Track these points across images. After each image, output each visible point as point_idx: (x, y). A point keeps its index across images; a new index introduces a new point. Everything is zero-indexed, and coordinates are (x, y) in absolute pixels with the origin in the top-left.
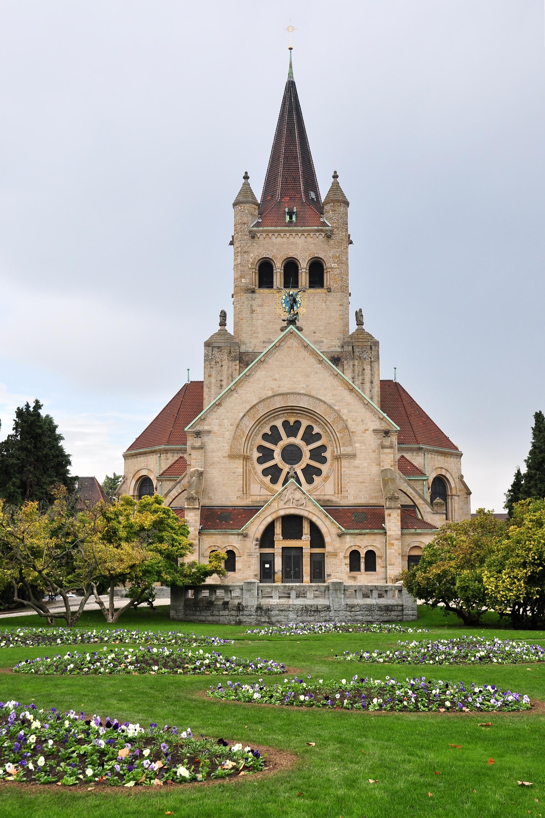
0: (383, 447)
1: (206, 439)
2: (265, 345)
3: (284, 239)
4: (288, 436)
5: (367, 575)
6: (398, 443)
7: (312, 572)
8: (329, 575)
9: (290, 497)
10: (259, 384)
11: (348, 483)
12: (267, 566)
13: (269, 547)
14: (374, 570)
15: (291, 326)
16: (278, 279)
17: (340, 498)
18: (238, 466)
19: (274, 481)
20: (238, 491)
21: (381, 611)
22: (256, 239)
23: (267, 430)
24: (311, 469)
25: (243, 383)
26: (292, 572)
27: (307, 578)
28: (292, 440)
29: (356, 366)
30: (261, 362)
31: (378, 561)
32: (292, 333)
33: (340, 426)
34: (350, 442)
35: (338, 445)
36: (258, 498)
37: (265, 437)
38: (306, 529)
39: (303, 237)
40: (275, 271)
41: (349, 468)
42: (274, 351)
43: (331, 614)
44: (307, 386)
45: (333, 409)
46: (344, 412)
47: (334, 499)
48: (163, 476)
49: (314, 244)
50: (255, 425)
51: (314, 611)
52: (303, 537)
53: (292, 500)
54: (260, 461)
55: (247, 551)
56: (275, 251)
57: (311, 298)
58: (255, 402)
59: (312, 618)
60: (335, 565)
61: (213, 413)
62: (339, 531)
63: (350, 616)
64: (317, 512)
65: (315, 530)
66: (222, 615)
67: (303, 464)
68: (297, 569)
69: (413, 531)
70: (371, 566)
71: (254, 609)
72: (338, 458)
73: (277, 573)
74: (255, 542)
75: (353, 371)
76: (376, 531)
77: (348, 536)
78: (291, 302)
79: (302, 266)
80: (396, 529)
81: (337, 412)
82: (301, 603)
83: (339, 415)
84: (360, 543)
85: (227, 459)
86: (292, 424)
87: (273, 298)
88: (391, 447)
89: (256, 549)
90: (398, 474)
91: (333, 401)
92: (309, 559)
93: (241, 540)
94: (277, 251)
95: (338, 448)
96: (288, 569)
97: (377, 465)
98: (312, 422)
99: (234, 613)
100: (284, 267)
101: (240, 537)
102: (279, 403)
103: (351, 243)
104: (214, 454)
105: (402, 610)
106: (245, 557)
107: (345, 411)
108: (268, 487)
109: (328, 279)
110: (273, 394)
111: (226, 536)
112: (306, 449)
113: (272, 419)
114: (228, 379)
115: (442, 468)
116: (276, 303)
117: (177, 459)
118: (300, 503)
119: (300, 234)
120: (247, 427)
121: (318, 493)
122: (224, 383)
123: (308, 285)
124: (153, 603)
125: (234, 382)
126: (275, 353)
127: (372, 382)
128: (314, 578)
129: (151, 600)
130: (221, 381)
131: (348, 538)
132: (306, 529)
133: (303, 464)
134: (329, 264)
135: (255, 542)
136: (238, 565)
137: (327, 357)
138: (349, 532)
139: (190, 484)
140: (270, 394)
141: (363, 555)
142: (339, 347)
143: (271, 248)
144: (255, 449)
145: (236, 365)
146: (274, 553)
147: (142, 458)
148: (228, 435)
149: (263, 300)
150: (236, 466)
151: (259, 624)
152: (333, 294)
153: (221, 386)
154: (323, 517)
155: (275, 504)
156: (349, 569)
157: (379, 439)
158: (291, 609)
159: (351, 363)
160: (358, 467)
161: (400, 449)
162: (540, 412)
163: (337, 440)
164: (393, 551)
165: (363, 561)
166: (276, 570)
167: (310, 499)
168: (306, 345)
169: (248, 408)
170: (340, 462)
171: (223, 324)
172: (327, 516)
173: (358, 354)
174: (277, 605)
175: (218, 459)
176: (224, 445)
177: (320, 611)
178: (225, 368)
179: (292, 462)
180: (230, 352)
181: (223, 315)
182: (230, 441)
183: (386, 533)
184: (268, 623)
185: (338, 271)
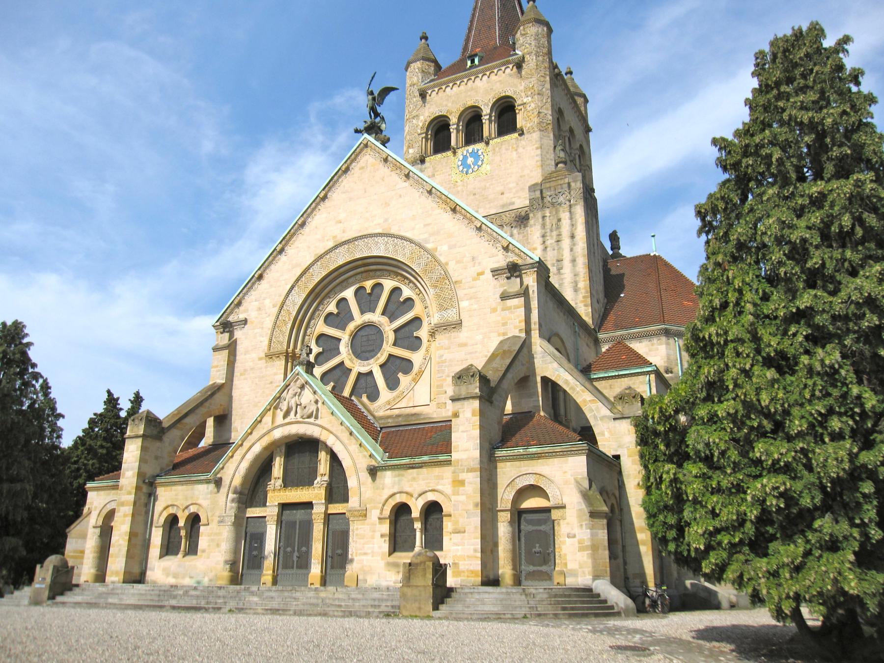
3: (463, 87)
4: (362, 312)
9: (293, 403)
23: (332, 308)
24: (398, 362)
27: (316, 569)
39: (485, 78)
41: (449, 348)
42: (340, 180)
44: (386, 220)
45: (425, 250)
49: (500, 81)
50: (309, 301)
55: (217, 514)
56: (450, 105)
57: (497, 149)
69: (521, 451)
74: (231, 496)
75: (544, 226)
77: (388, 474)
81: (431, 254)
83: (433, 257)
85: (264, 361)
87: (447, 163)
91: (426, 236)
94: (452, 103)
96: (289, 549)
102: (342, 258)
106: (214, 525)
111: (190, 487)
113: (337, 289)
116: (451, 168)
121: (402, 404)
128: (332, 567)
131: (388, 478)
135: (231, 496)
136: (203, 543)
140: (331, 244)
141: (416, 513)
143: (445, 103)
148: (269, 323)
149: (434, 169)
152: (526, 136)
154: (345, 436)
159: (539, 215)
160: (465, 345)
166: (266, 553)
173: (549, 199)
179: (367, 355)
185: (533, 105)
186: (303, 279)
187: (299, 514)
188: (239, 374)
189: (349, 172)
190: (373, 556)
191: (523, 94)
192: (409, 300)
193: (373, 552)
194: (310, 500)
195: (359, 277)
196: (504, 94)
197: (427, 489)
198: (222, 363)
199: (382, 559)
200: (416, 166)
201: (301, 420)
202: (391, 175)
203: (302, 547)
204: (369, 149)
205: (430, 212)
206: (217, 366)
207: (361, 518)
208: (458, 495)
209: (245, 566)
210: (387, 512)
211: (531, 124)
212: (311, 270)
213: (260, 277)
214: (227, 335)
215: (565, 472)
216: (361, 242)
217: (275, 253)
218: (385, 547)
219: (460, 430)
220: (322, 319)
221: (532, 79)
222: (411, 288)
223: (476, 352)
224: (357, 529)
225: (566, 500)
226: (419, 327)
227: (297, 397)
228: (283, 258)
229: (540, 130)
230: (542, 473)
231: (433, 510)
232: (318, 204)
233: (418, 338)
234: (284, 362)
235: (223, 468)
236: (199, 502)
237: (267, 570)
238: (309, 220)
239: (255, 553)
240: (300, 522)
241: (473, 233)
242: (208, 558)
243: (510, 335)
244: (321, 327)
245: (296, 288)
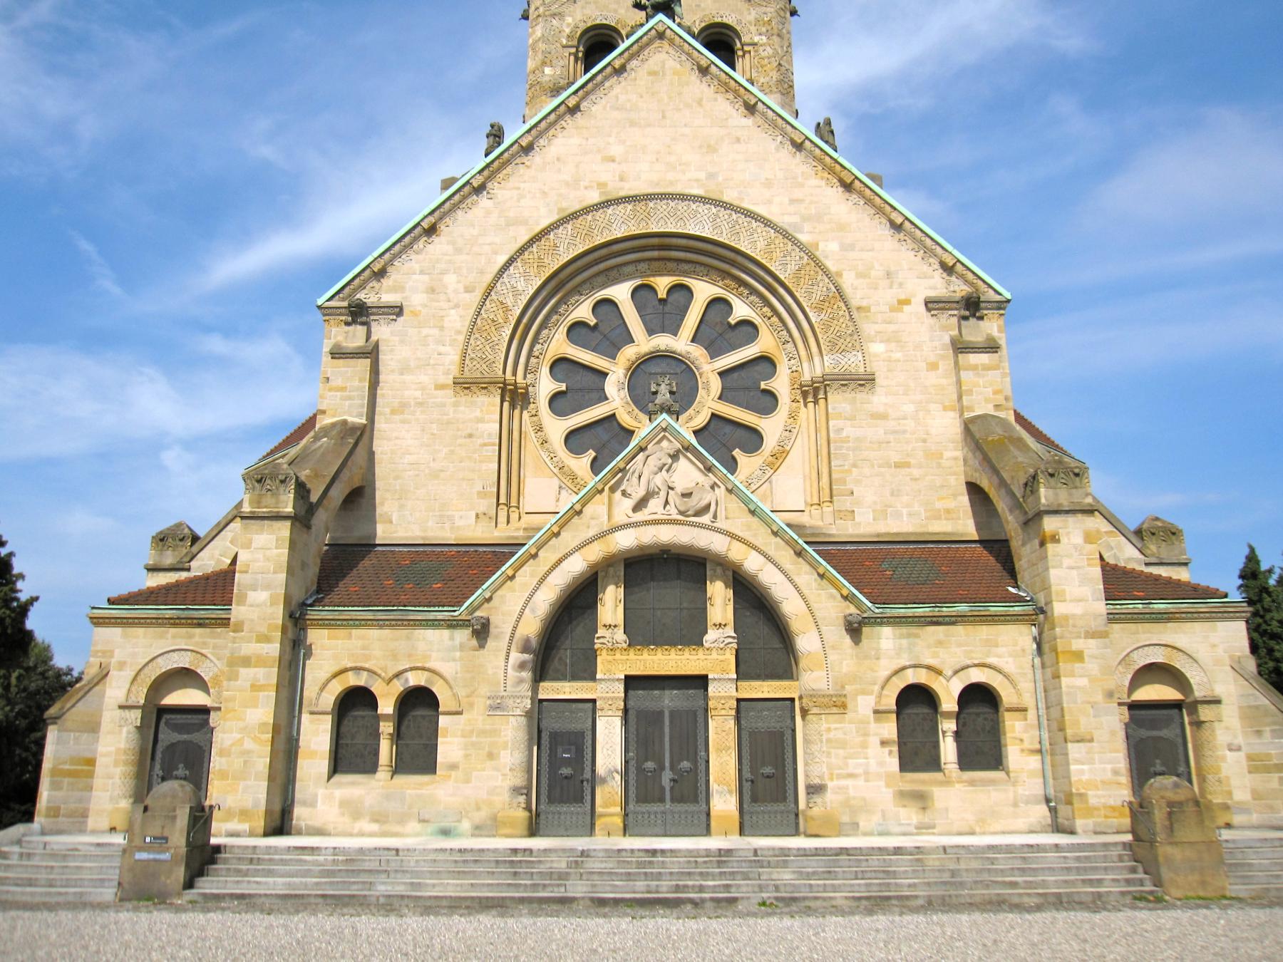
1: (382, 331)
4: (651, 331)
5: (972, 783)
7: (747, 775)
8: (815, 790)
9: (659, 480)
10: (559, 171)
11: (855, 466)
13: (575, 677)
17: (829, 519)
20: (482, 494)
23: (583, 311)
24: (728, 429)
25: (509, 169)
26: (667, 776)
27: (724, 802)
28: (663, 341)
32: (661, 36)
33: (822, 287)
34: (853, 339)
41: (852, 418)
42: (607, 84)
44: (711, 176)
45: (796, 243)
46: (829, 251)
50: (544, 293)
52: (711, 636)
53: (663, 494)
55: (484, 690)
58: (545, 223)
60: (842, 744)
61: (413, 256)
62: (852, 610)
68: (685, 764)
69: (1139, 606)
72: (812, 392)
73: (604, 781)
74: (516, 656)
76: (995, 609)
77: (887, 631)
80: (1086, 591)
83: (812, 257)
84: (935, 655)
85: (450, 392)
86: (662, 294)
89: (521, 681)
92: (731, 723)
93: (462, 647)
96: (650, 765)
98: (726, 287)
101: (463, 635)
102: (620, 225)
104: (408, 378)
106: (476, 716)
110: (604, 199)
111: (402, 633)
112: (709, 369)
113: (601, 279)
118: (696, 502)
120: (516, 293)
128: (755, 799)
131: (886, 639)
135: (516, 656)
136: (448, 748)
138: (889, 612)
140: (594, 197)
141: (949, 703)
144: (545, 370)
146: (594, 701)
148: (458, 321)
150: (478, 413)
157: (945, 328)
160: (883, 417)
164: (1083, 682)
166: (601, 768)
169: (525, 238)
170: (822, 402)
175: (418, 394)
176: (442, 349)
182: (461, 338)
185: (769, 51)
186: (534, 249)
187: (669, 699)
188: (387, 410)
189: (625, 75)
190: (867, 780)
191: (753, 29)
192: (746, 323)
193: (867, 773)
194: (704, 673)
196: (719, 20)
197: (969, 662)
198: (356, 383)
199: (887, 785)
200: (772, 96)
201: (680, 517)
202: (716, 100)
203: (646, 760)
204: (665, 43)
205: (800, 180)
206: (343, 389)
207: (835, 710)
208: (1074, 676)
209: (544, 798)
210: (891, 702)
211: (767, 79)
212: (552, 236)
213: (431, 231)
214: (361, 330)
215: (1214, 646)
216: (662, 205)
217: (467, 189)
218: (894, 762)
219: (1065, 565)
220: (563, 330)
221: (768, 10)
223: (904, 432)
224: (829, 730)
225: (1220, 690)
227: (664, 472)
228: (483, 202)
229: (783, 94)
230: (1177, 645)
232: (560, 117)
233: (770, 394)
234: (498, 400)
235: (489, 600)
237: (606, 805)
238: (542, 142)
239: (566, 771)
240: (672, 713)
241: (887, 231)
242: (468, 781)
244: (559, 344)
245: (519, 263)
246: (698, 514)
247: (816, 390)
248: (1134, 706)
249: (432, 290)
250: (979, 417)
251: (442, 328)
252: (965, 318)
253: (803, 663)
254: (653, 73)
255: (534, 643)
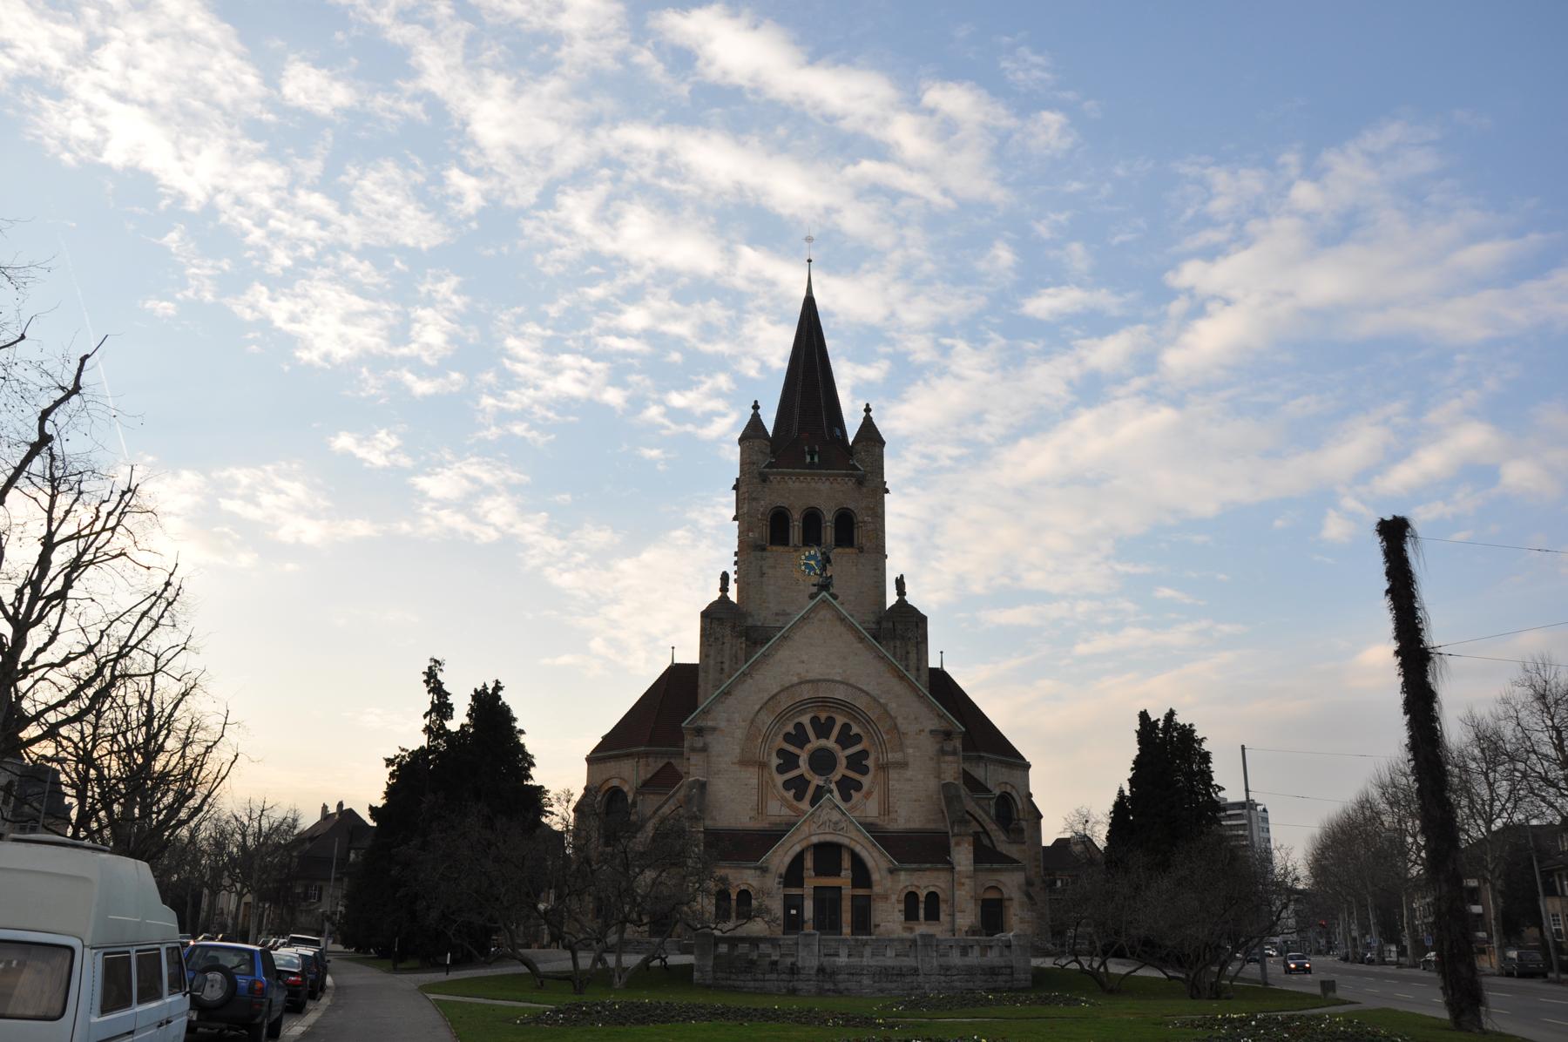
0: (943, 752)
1: (709, 738)
2: (777, 618)
3: (804, 485)
6: (963, 750)
8: (877, 926)
12: (793, 912)
14: (937, 919)
15: (824, 593)
16: (795, 534)
17: (886, 822)
18: (751, 776)
19: (799, 797)
20: (751, 809)
21: (985, 974)
22: (768, 483)
23: (790, 728)
26: (827, 920)
27: (846, 930)
28: (823, 742)
29: (898, 650)
30: (784, 638)
31: (943, 907)
32: (824, 602)
34: (901, 747)
35: (884, 750)
36: (778, 820)
37: (788, 738)
38: (846, 862)
39: (828, 483)
40: (791, 524)
43: (921, 979)
46: (892, 706)
47: (877, 821)
48: (647, 786)
51: (897, 975)
52: (843, 873)
54: (781, 769)
56: (792, 498)
59: (893, 985)
63: (944, 982)
64: (861, 840)
65: (859, 864)
66: (768, 980)
67: (837, 776)
69: (988, 866)
70: (933, 915)
71: (813, 972)
72: (884, 767)
73: (806, 922)
74: (777, 880)
76: (939, 866)
77: (903, 873)
78: (824, 562)
79: (827, 519)
81: (884, 707)
82: (880, 964)
88: (954, 753)
89: (779, 888)
90: (964, 791)
92: (850, 904)
93: (759, 877)
95: (885, 755)
97: (935, 777)
99: (784, 976)
100: (804, 519)
101: (758, 872)
102: (807, 693)
103: (887, 491)
104: (720, 759)
105: (1012, 974)
107: (894, 705)
108: (792, 805)
109: (859, 536)
112: (842, 755)
113: (798, 714)
114: (731, 660)
115: (1006, 783)
116: (793, 564)
117: (661, 765)
119: (824, 479)
121: (857, 814)
122: (726, 666)
123: (833, 543)
124: (667, 960)
125: (748, 664)
126: (802, 627)
127: (918, 670)
129: (663, 956)
130: (722, 663)
131: (903, 876)
132: (846, 862)
133: (837, 776)
134: (862, 517)
135: (777, 880)
137: (869, 633)
139: (688, 800)
140: (795, 680)
141: (922, 899)
142: (874, 623)
144: (774, 754)
145: (741, 643)
146: (803, 895)
147: (613, 763)
148: (739, 734)
149: (776, 560)
150: (749, 775)
151: (821, 992)
153: (722, 669)
154: (869, 846)
155: (805, 828)
156: (903, 917)
158: (865, 972)
159: (892, 644)
160: (911, 780)
161: (966, 759)
162: (1146, 711)
163: (882, 743)
164: (964, 893)
165: (922, 906)
166: (806, 917)
167: (852, 822)
168: (842, 617)
171: (724, 588)
172: (875, 845)
174: (846, 966)
177: (904, 975)
178: (727, 646)
180: (734, 627)
181: (725, 577)
183: (953, 868)
184: (834, 991)
192: (858, 735)
195: (815, 709)
206: (696, 765)
222: (860, 726)
225: (1013, 895)
226: (867, 758)
231: (933, 898)
233: (867, 767)
236: (749, 882)
243: (947, 781)
244: (780, 742)
246: (840, 830)
247: (884, 768)
248: (984, 901)
249: (728, 721)
250: (948, 783)
251: (733, 738)
252: (945, 740)
253: (874, 884)
254: (820, 620)
255: (784, 875)
